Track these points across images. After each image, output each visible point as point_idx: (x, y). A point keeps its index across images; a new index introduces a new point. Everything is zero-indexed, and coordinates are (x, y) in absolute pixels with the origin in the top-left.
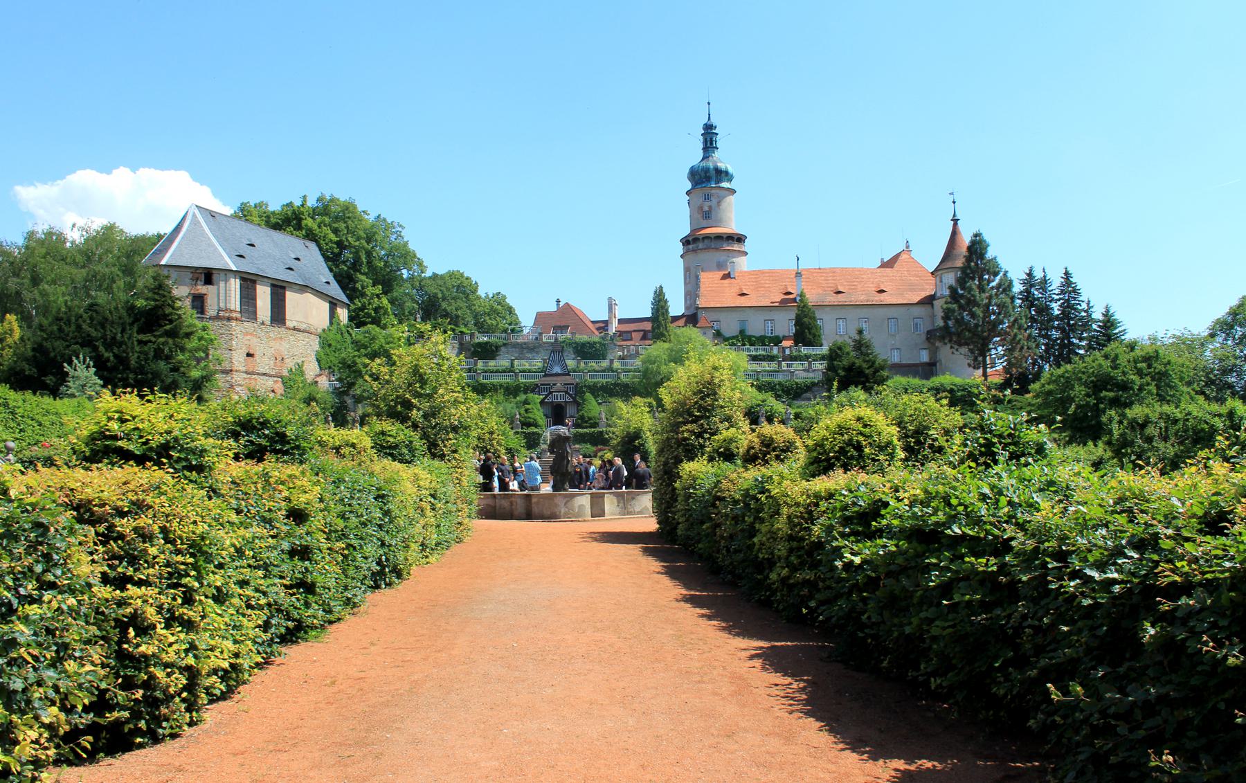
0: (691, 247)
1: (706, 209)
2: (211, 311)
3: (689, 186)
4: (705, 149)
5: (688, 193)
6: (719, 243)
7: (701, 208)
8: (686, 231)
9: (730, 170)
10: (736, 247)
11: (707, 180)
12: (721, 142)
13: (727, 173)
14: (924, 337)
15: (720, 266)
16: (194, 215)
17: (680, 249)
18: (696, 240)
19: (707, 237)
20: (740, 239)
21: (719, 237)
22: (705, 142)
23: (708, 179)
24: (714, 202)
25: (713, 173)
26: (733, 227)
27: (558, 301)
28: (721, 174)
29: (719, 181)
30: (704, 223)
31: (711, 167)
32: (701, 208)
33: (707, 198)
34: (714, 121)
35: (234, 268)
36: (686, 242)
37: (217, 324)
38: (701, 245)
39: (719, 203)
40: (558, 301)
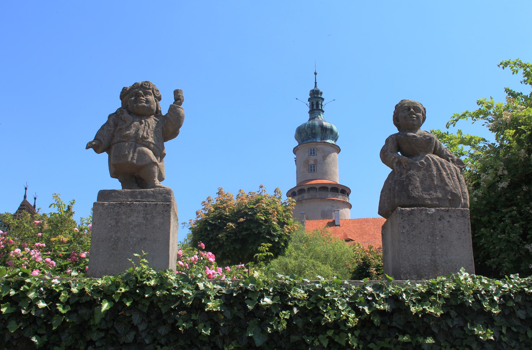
1: (312, 162)
3: (296, 144)
5: (295, 150)
6: (323, 194)
8: (293, 184)
9: (335, 128)
10: (340, 198)
12: (326, 106)
13: (331, 130)
15: (324, 215)
19: (312, 188)
20: (345, 191)
21: (324, 188)
22: (312, 105)
23: (314, 135)
24: (319, 156)
25: (319, 130)
26: (339, 179)
29: (324, 138)
30: (310, 176)
31: (317, 123)
32: (307, 162)
33: (313, 152)
34: (320, 88)
38: (306, 195)
39: (325, 157)
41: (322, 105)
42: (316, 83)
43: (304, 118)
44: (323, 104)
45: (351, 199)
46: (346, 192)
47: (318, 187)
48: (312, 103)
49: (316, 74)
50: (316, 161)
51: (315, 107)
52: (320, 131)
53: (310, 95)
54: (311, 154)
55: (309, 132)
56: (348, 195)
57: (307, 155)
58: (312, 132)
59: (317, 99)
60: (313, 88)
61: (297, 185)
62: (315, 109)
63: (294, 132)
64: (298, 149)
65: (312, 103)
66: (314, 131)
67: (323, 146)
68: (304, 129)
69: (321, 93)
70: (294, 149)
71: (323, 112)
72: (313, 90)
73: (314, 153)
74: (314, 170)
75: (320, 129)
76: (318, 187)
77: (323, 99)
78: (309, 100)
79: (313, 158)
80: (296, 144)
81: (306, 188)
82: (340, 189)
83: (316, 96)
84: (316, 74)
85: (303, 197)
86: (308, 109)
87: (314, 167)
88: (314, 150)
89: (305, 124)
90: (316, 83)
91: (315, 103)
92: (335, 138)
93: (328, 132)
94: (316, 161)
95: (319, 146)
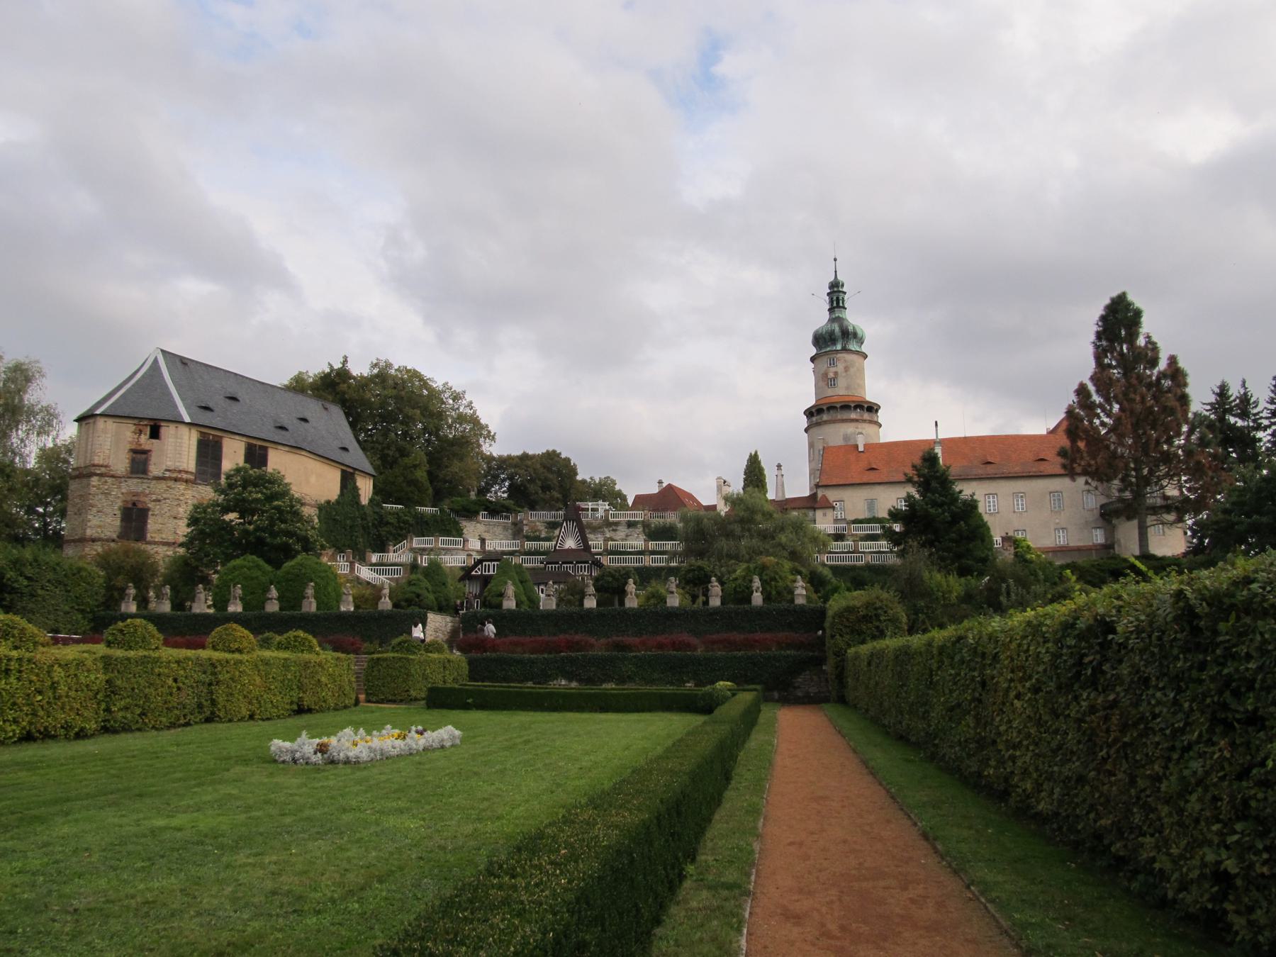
1: (831, 375)
2: (155, 470)
3: (813, 351)
4: (831, 310)
5: (813, 359)
7: (825, 375)
8: (811, 401)
10: (866, 416)
11: (834, 341)
13: (855, 335)
14: (1097, 513)
16: (156, 361)
17: (804, 422)
19: (831, 408)
21: (846, 407)
22: (831, 301)
24: (840, 367)
27: (660, 482)
28: (849, 335)
33: (833, 363)
35: (187, 420)
36: (809, 413)
37: (162, 486)
38: (825, 417)
40: (660, 482)
43: (820, 318)
45: (882, 416)
50: (836, 373)
56: (877, 411)
60: (832, 279)
63: (810, 338)
79: (833, 369)
80: (813, 351)
86: (828, 307)
92: (861, 341)
94: (836, 373)
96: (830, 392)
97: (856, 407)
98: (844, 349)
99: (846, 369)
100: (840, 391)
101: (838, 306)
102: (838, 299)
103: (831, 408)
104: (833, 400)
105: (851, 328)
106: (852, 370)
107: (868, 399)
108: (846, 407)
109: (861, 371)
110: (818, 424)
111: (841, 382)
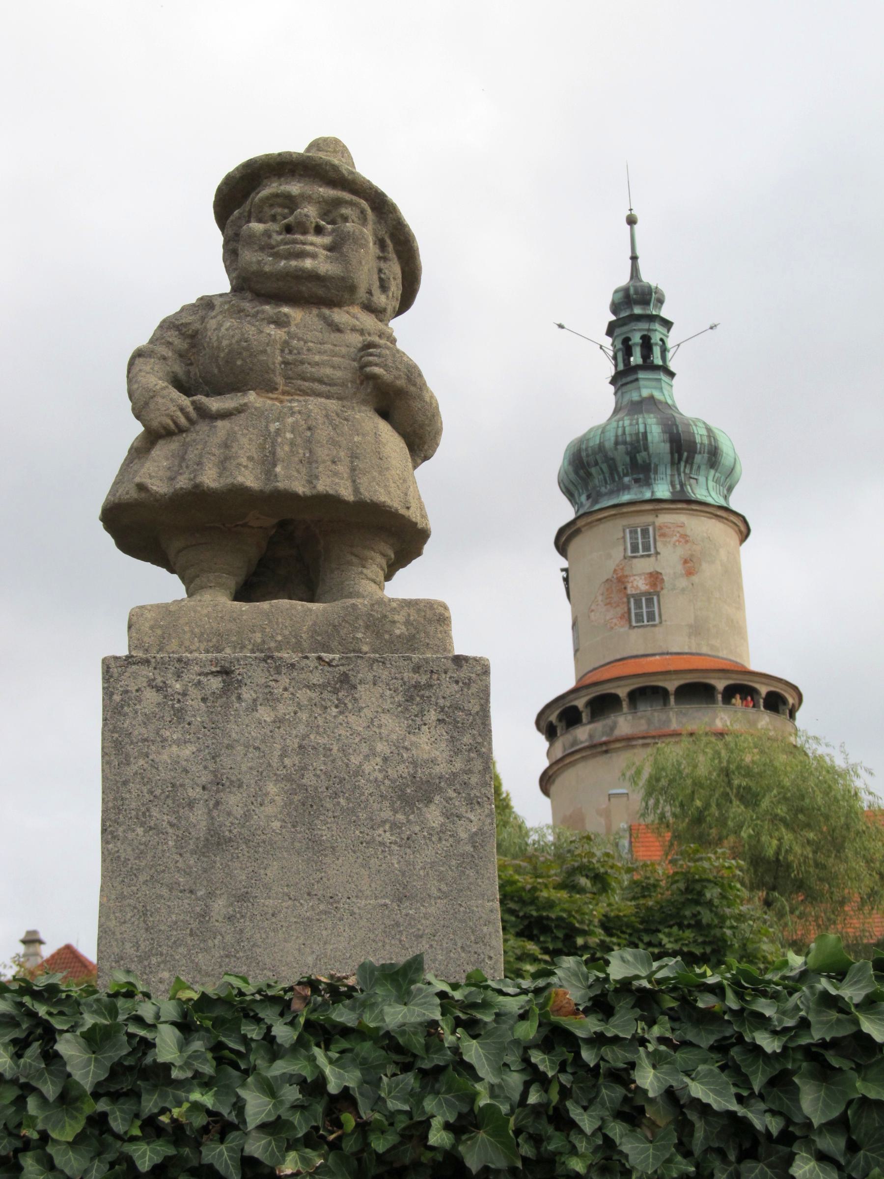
0: (582, 733)
1: (640, 584)
4: (623, 377)
5: (563, 541)
7: (620, 581)
12: (682, 349)
13: (714, 456)
18: (603, 705)
19: (648, 694)
21: (697, 692)
22: (627, 349)
24: (668, 559)
32: (620, 581)
33: (643, 544)
34: (648, 277)
38: (624, 723)
41: (664, 350)
42: (634, 258)
44: (670, 343)
46: (784, 701)
47: (671, 686)
48: (626, 341)
49: (631, 221)
51: (636, 359)
52: (668, 458)
53: (615, 308)
54: (635, 549)
55: (621, 456)
56: (792, 715)
57: (617, 554)
58: (633, 459)
59: (644, 325)
60: (623, 279)
61: (579, 680)
62: (637, 368)
64: (578, 532)
65: (626, 341)
66: (641, 457)
67: (682, 518)
68: (601, 448)
69: (660, 301)
70: (561, 531)
71: (672, 375)
72: (626, 290)
73: (647, 548)
74: (651, 616)
75: (665, 448)
76: (671, 686)
77: (668, 324)
78: (611, 330)
79: (643, 565)
80: (566, 512)
81: (622, 692)
82: (764, 690)
83: (638, 310)
84: (631, 221)
85: (613, 728)
86: (609, 370)
87: (650, 602)
88: (645, 532)
89: (603, 429)
90: (634, 258)
91: (636, 339)
92: (728, 483)
93: (698, 458)
94: (655, 578)
95: (665, 519)
96: (636, 642)
97: (730, 693)
98: (683, 501)
99: (690, 566)
100: (672, 641)
101: (648, 366)
102: (647, 344)
103: (648, 694)
104: (648, 665)
105: (700, 434)
106: (708, 571)
107: (755, 666)
108: (697, 692)
109: (732, 574)
110: (600, 749)
111: (675, 608)
